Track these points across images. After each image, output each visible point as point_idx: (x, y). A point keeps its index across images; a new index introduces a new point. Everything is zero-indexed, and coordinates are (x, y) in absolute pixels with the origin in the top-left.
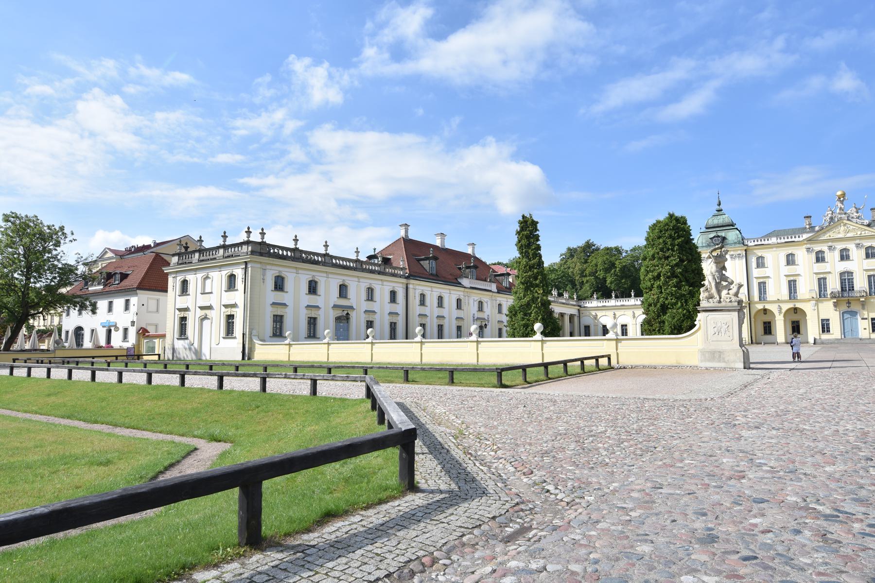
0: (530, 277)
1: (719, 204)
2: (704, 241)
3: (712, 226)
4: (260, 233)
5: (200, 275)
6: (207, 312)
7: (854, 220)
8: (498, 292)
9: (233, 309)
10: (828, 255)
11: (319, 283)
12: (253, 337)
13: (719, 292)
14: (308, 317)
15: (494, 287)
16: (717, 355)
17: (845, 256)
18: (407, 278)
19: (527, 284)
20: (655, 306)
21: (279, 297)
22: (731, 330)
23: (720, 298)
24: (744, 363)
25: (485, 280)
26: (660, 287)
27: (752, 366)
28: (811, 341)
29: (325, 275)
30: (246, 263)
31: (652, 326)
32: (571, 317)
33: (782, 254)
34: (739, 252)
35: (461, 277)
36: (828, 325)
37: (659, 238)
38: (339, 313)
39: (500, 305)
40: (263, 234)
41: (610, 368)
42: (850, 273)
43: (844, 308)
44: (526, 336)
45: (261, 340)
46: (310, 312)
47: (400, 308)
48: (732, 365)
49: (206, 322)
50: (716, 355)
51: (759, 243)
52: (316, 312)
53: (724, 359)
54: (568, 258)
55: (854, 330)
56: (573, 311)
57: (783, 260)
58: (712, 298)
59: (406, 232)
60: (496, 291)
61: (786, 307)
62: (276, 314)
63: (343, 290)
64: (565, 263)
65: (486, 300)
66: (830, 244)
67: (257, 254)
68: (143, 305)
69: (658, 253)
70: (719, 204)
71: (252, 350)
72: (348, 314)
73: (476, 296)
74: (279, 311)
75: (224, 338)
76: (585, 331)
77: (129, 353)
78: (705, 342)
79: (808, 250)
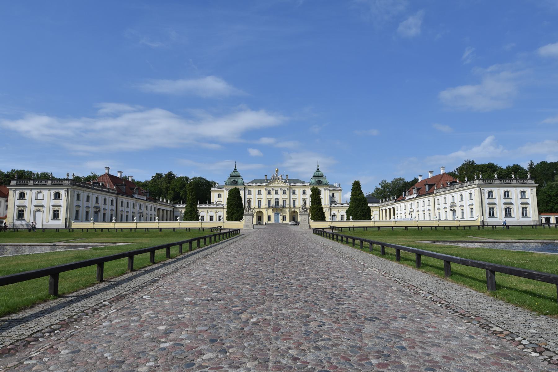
1: (235, 167)
4: (73, 176)
5: (34, 192)
6: (41, 208)
7: (280, 180)
8: (147, 201)
9: (59, 208)
10: (272, 192)
12: (71, 220)
17: (277, 193)
18: (118, 194)
28: (264, 223)
30: (68, 189)
32: (171, 211)
33: (257, 190)
35: (135, 193)
36: (270, 218)
38: (95, 210)
39: (147, 206)
42: (278, 199)
43: (275, 212)
49: (38, 213)
50: (247, 226)
51: (249, 185)
54: (157, 179)
55: (278, 220)
56: (171, 209)
57: (257, 193)
59: (108, 171)
61: (257, 210)
64: (155, 182)
66: (272, 188)
70: (235, 167)
73: (139, 202)
79: (265, 189)
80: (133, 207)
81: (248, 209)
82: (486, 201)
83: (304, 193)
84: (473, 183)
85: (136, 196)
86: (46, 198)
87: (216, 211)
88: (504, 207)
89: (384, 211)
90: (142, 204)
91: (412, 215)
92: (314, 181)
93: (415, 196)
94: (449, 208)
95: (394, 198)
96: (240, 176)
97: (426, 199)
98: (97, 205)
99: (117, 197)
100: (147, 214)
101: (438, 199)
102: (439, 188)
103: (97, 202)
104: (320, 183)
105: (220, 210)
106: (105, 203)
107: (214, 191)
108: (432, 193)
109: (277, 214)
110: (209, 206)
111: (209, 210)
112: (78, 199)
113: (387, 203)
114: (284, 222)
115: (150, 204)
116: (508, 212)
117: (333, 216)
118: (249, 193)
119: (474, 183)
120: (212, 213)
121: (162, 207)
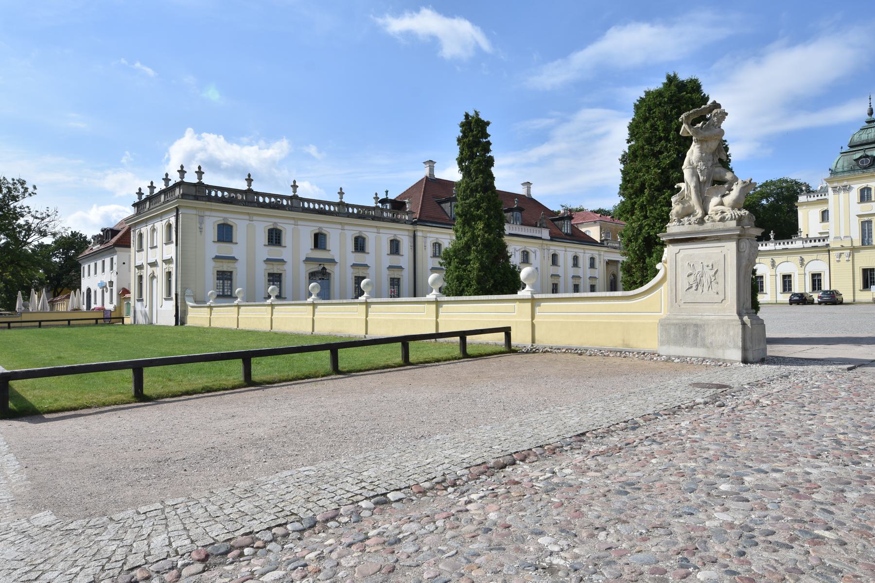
0: (470, 206)
2: (845, 164)
3: (859, 143)
8: (551, 240)
11: (401, 243)
12: (187, 299)
13: (704, 203)
14: (355, 277)
15: (545, 234)
16: (690, 332)
19: (466, 216)
20: (636, 240)
21: (225, 249)
22: (720, 280)
23: (705, 213)
24: (744, 349)
25: (536, 226)
26: (643, 208)
27: (773, 350)
29: (292, 222)
30: (177, 209)
31: (631, 275)
37: (646, 120)
38: (315, 267)
39: (554, 257)
40: (200, 173)
41: (509, 349)
44: (461, 295)
45: (196, 302)
46: (271, 266)
47: (405, 259)
48: (719, 354)
52: (280, 267)
53: (703, 339)
58: (689, 215)
59: (432, 170)
60: (549, 238)
62: (271, 271)
63: (319, 240)
65: (533, 249)
67: (191, 197)
68: (124, 263)
69: (642, 148)
71: (185, 312)
72: (324, 268)
74: (225, 267)
75: (165, 299)
77: (106, 316)
78: (672, 306)
81: (700, 187)
87: (802, 260)
99: (414, 231)
105: (814, 256)
107: (808, 204)
110: (778, 247)
111: (778, 260)
120: (789, 265)
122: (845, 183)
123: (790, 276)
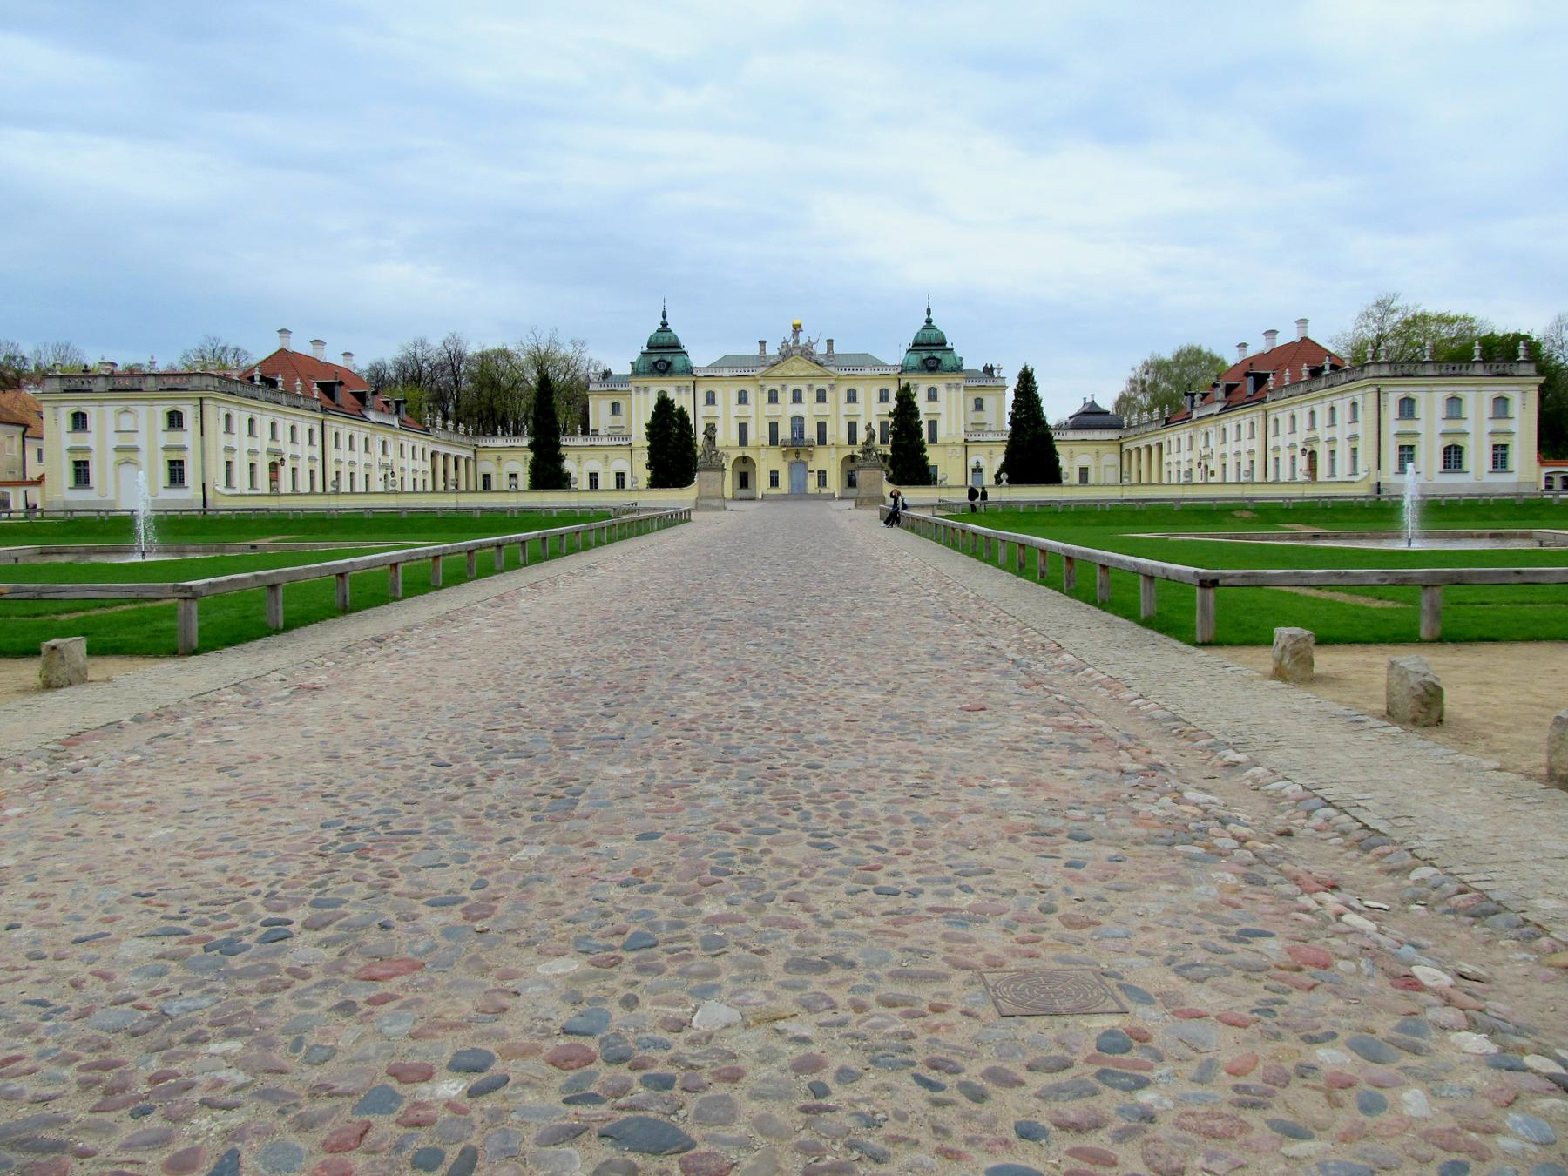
1: (664, 316)
15: (395, 422)
17: (797, 397)
18: (324, 410)
30: (201, 399)
34: (687, 383)
42: (801, 419)
43: (792, 458)
47: (317, 453)
57: (734, 398)
70: (664, 316)
76: (484, 482)
80: (367, 450)
82: (1392, 425)
83: (884, 397)
84: (1362, 371)
85: (372, 416)
86: (143, 428)
87: (607, 458)
88: (1439, 445)
89: (1134, 454)
90: (389, 439)
91: (1207, 467)
92: (915, 360)
93: (1217, 407)
94: (1300, 447)
95: (1162, 412)
96: (679, 347)
97: (1246, 418)
98: (274, 445)
100: (402, 469)
101: (1276, 420)
102: (1280, 386)
103: (273, 437)
104: (931, 366)
106: (293, 440)
108: (1262, 401)
109: (798, 467)
112: (228, 429)
113: (1142, 429)
114: (824, 491)
115: (411, 440)
116: (1453, 457)
117: (974, 470)
118: (711, 399)
119: (1365, 375)
121: (443, 450)
122: (646, 384)
123: (596, 474)
